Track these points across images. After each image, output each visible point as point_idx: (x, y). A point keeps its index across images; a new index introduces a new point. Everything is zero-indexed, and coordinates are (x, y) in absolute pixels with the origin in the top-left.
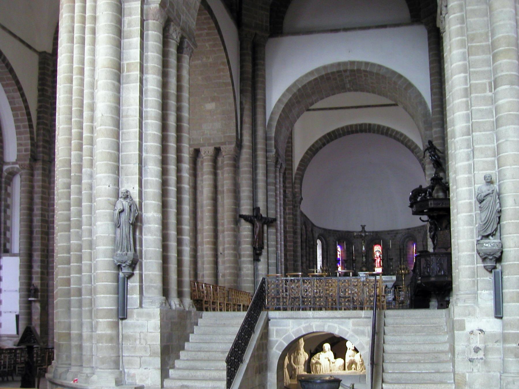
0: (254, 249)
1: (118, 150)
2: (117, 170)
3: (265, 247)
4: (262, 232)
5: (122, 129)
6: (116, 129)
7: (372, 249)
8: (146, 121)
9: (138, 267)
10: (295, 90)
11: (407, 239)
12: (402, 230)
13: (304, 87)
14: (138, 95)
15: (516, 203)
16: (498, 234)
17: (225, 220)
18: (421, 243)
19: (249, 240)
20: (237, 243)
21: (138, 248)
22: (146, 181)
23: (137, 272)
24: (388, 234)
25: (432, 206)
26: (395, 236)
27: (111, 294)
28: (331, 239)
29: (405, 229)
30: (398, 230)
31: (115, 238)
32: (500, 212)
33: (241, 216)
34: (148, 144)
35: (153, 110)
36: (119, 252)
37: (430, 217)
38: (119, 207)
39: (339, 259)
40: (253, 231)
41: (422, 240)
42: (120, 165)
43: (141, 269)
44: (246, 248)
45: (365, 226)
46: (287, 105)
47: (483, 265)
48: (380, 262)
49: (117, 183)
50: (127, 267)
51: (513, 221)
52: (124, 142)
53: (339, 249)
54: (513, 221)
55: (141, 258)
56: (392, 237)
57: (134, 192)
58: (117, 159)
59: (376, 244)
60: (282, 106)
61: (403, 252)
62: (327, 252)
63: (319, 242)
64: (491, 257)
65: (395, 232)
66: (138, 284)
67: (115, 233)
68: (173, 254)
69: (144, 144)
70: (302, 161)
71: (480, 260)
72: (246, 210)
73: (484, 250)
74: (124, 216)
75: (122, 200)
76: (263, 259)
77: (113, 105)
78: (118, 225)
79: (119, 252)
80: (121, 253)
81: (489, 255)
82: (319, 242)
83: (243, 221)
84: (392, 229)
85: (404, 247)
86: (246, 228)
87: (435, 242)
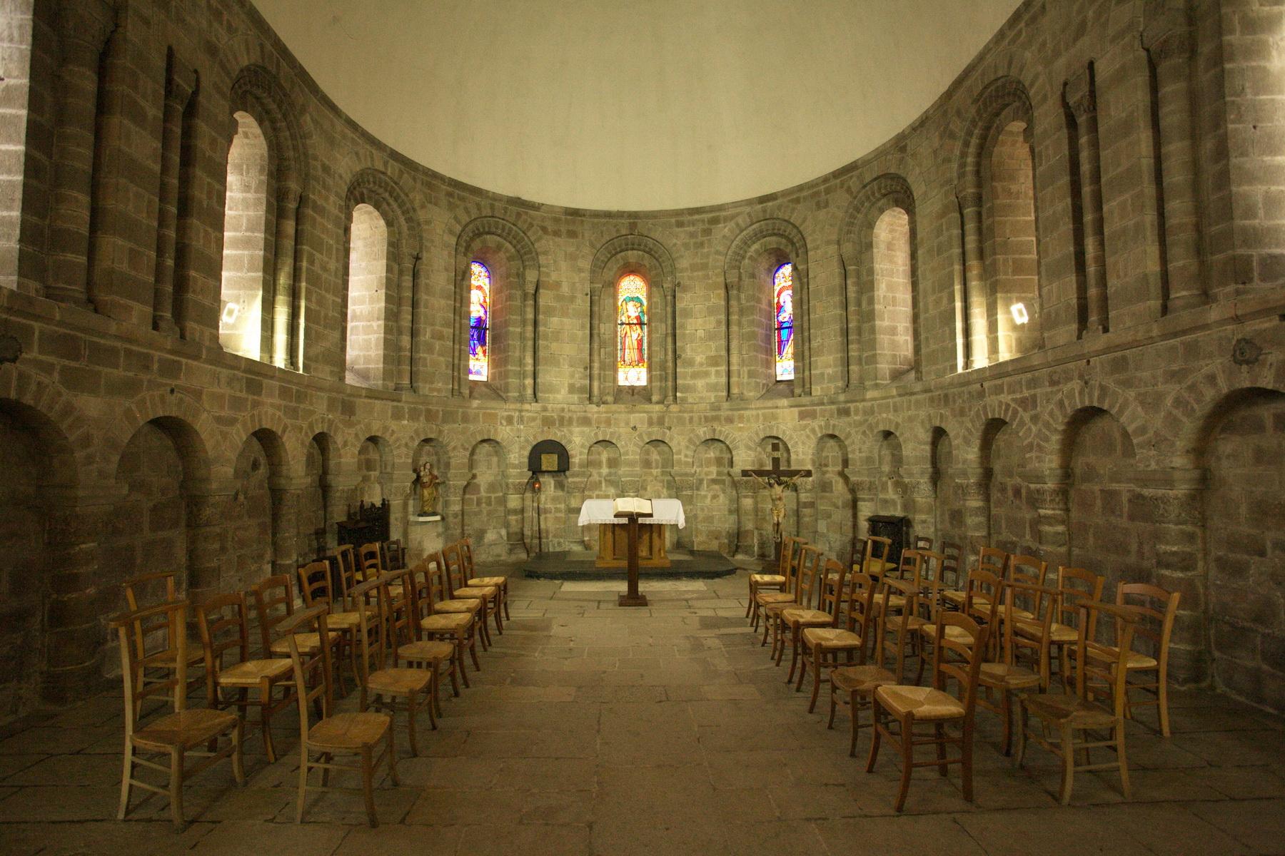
7: (613, 285)
12: (736, 204)
18: (833, 249)
24: (680, 224)
26: (707, 232)
29: (749, 202)
30: (720, 208)
48: (640, 342)
56: (692, 235)
59: (630, 269)
61: (739, 299)
62: (415, 276)
65: (706, 216)
85: (740, 278)
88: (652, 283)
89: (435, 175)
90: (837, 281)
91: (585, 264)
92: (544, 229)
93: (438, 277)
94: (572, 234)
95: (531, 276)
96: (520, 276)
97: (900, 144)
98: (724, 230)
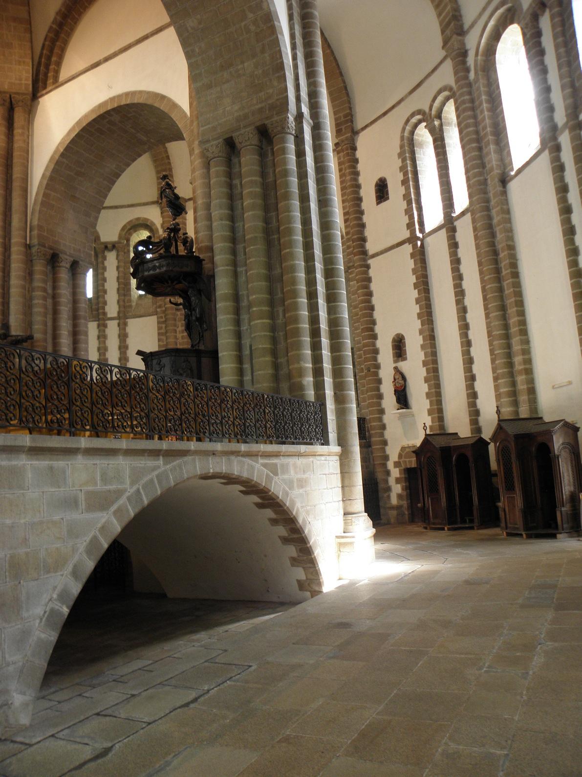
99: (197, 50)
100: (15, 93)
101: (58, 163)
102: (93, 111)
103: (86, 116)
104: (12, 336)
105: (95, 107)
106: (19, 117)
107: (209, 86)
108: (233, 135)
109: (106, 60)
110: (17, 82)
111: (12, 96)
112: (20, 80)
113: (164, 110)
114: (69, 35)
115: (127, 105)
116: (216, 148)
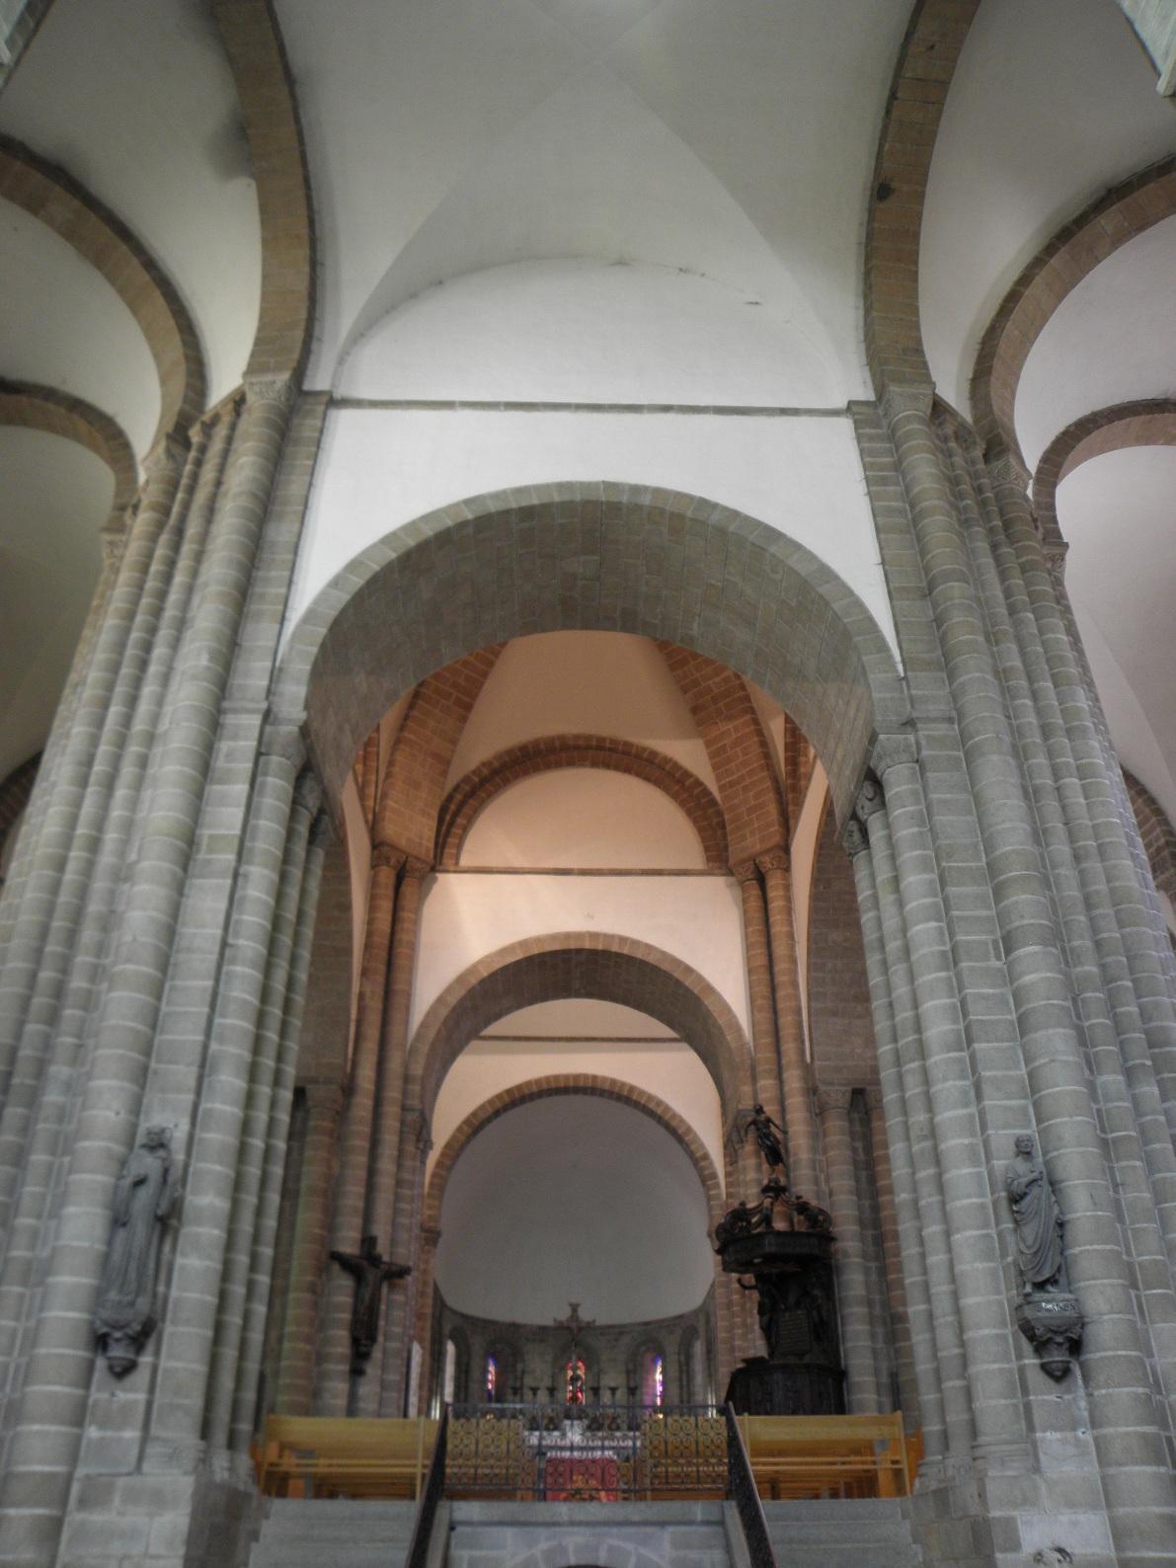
0: (355, 1341)
1: (154, 1026)
2: (142, 1076)
3: (380, 1339)
4: (375, 1300)
5: (173, 979)
6: (159, 975)
8: (232, 968)
9: (150, 1346)
10: (474, 981)
11: (644, 1348)
12: (633, 1325)
13: (493, 975)
14: (223, 905)
15: (1095, 1204)
16: (1062, 1280)
17: (295, 1263)
18: (676, 1357)
19: (346, 1316)
20: (319, 1323)
21: (161, 1289)
22: (209, 1112)
23: (146, 1359)
25: (773, 1249)
27: (62, 1423)
28: (477, 1344)
29: (639, 1324)
31: (106, 1257)
32: (1061, 1225)
33: (336, 1257)
34: (229, 1021)
35: (251, 944)
36: (113, 1295)
37: (758, 1277)
38: (135, 1170)
39: (489, 1391)
40: (357, 1297)
41: (677, 1350)
42: (153, 1065)
43: (157, 1353)
44: (340, 1341)
45: (578, 1305)
46: (454, 1010)
47: (1036, 1361)
49: (136, 1108)
50: (124, 1343)
51: (1096, 1247)
52: (172, 1009)
53: (492, 1368)
54: (1096, 1247)
55: (163, 1320)
57: (179, 1136)
58: (147, 1050)
60: (444, 1012)
63: (450, 1348)
64: (1060, 1339)
66: (141, 1397)
67: (110, 1243)
68: (235, 1319)
69: (217, 1021)
70: (448, 1146)
71: (1027, 1347)
72: (348, 1243)
73: (1046, 1318)
74: (145, 1195)
75: (143, 1152)
76: (372, 1369)
77: (163, 918)
78: (119, 1220)
79: (113, 1295)
80: (117, 1298)
81: (1055, 1332)
82: (450, 1348)
83: (336, 1267)
84: (610, 1322)
86: (342, 1291)
87: (773, 1340)
88: (588, 1368)
89: (478, 1319)
90: (677, 1374)
91: (549, 1358)
92: (527, 1340)
93: (476, 1374)
94: (542, 1341)
95: (520, 1366)
96: (514, 1366)
97: (696, 1313)
98: (625, 1340)
99: (830, 965)
100: (418, 858)
101: (471, 991)
102: (554, 937)
103: (538, 940)
104: (385, 1263)
105: (559, 934)
106: (408, 889)
107: (834, 1014)
108: (869, 1088)
109: (584, 872)
110: (417, 840)
111: (409, 859)
112: (421, 839)
113: (691, 987)
114: (490, 796)
115: (619, 955)
116: (837, 1095)
